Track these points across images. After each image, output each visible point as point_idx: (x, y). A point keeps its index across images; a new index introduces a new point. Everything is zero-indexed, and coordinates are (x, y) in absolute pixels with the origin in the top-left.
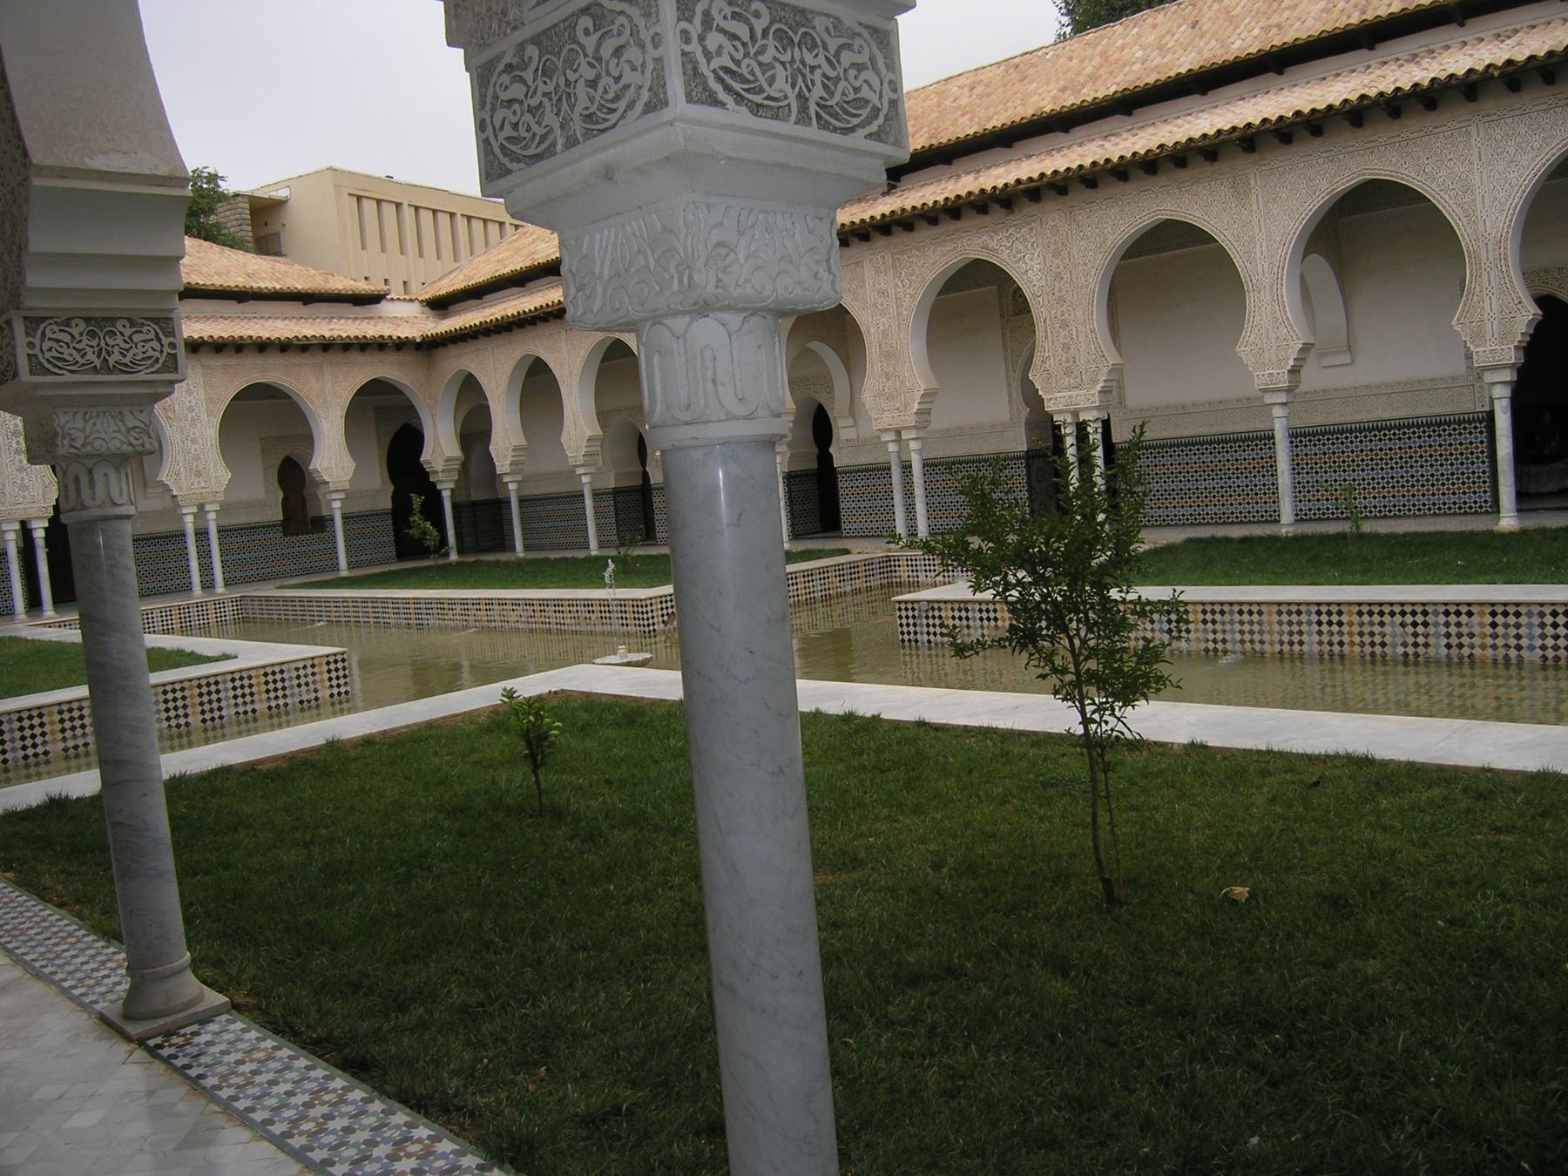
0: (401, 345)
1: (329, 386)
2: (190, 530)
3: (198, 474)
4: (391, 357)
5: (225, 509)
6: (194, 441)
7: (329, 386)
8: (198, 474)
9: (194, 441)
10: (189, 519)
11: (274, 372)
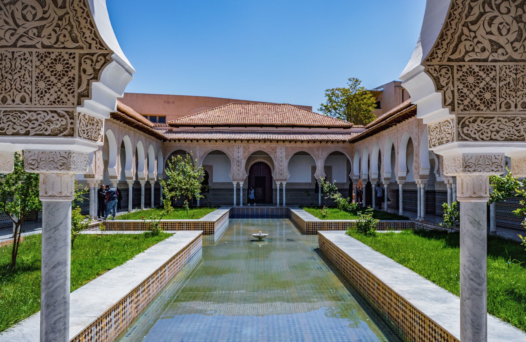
0: (344, 141)
1: (320, 153)
2: (278, 188)
3: (281, 175)
4: (341, 144)
5: (287, 184)
6: (281, 166)
7: (320, 153)
8: (281, 175)
9: (281, 166)
10: (278, 186)
11: (305, 147)
